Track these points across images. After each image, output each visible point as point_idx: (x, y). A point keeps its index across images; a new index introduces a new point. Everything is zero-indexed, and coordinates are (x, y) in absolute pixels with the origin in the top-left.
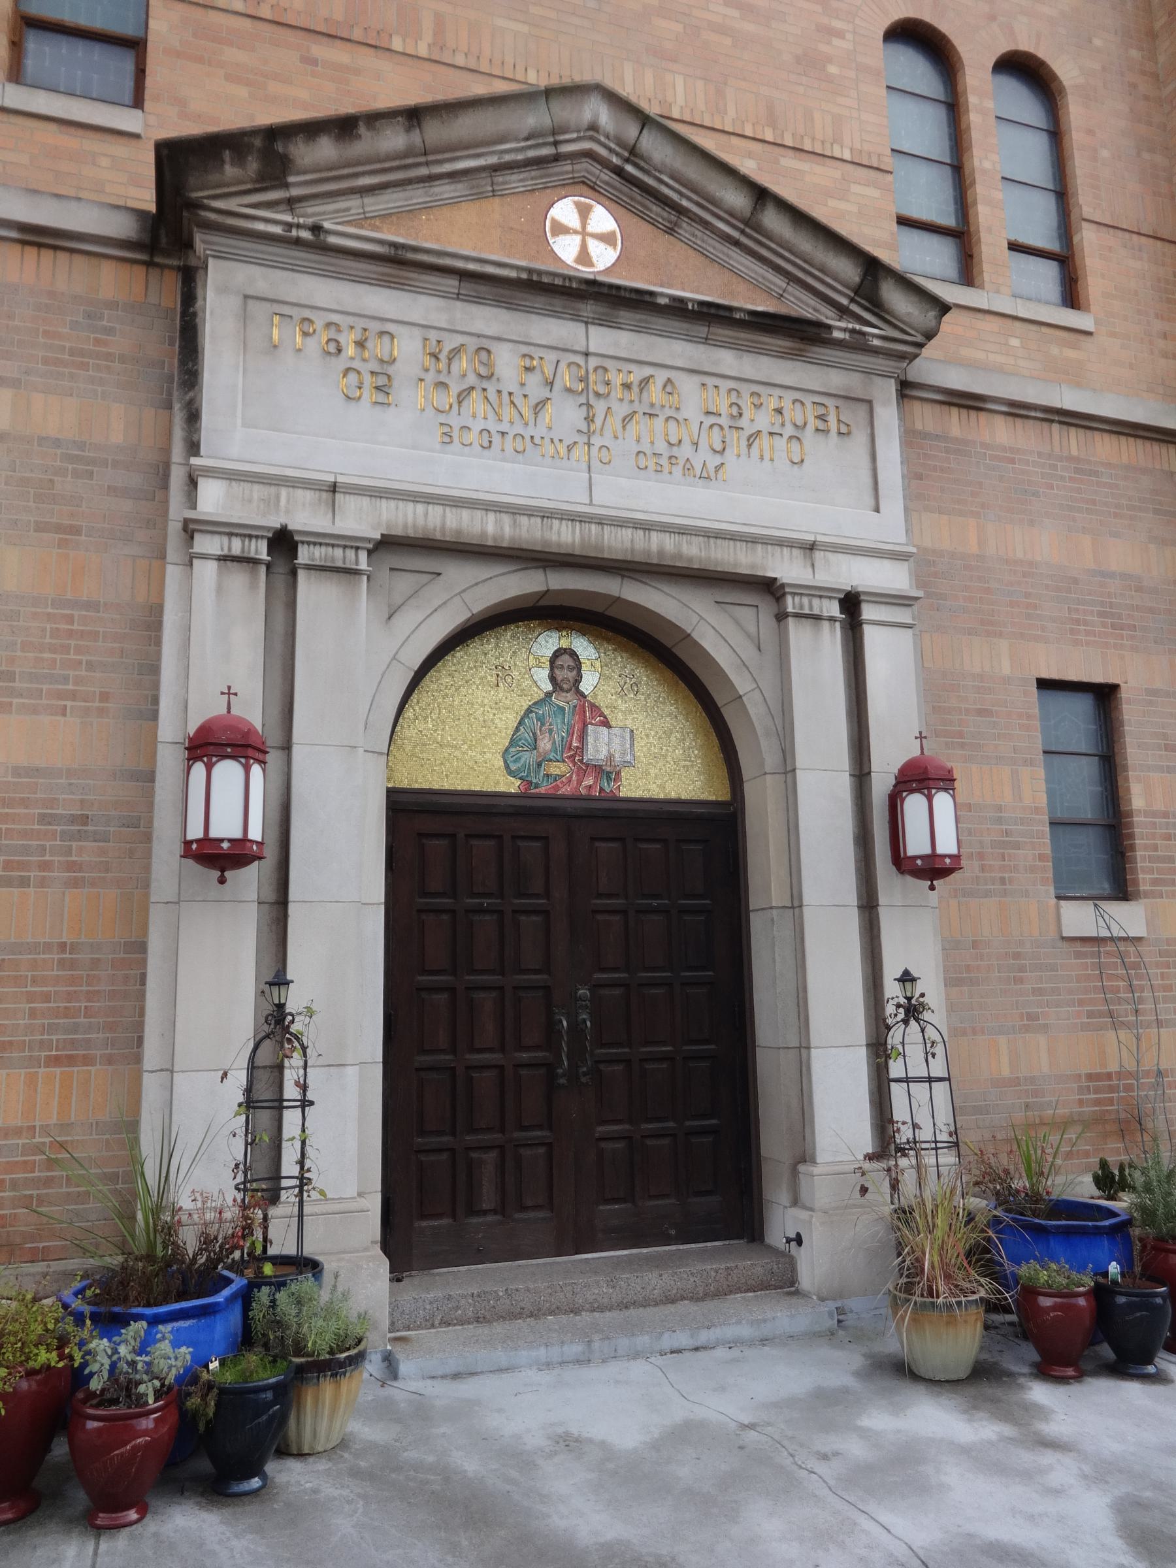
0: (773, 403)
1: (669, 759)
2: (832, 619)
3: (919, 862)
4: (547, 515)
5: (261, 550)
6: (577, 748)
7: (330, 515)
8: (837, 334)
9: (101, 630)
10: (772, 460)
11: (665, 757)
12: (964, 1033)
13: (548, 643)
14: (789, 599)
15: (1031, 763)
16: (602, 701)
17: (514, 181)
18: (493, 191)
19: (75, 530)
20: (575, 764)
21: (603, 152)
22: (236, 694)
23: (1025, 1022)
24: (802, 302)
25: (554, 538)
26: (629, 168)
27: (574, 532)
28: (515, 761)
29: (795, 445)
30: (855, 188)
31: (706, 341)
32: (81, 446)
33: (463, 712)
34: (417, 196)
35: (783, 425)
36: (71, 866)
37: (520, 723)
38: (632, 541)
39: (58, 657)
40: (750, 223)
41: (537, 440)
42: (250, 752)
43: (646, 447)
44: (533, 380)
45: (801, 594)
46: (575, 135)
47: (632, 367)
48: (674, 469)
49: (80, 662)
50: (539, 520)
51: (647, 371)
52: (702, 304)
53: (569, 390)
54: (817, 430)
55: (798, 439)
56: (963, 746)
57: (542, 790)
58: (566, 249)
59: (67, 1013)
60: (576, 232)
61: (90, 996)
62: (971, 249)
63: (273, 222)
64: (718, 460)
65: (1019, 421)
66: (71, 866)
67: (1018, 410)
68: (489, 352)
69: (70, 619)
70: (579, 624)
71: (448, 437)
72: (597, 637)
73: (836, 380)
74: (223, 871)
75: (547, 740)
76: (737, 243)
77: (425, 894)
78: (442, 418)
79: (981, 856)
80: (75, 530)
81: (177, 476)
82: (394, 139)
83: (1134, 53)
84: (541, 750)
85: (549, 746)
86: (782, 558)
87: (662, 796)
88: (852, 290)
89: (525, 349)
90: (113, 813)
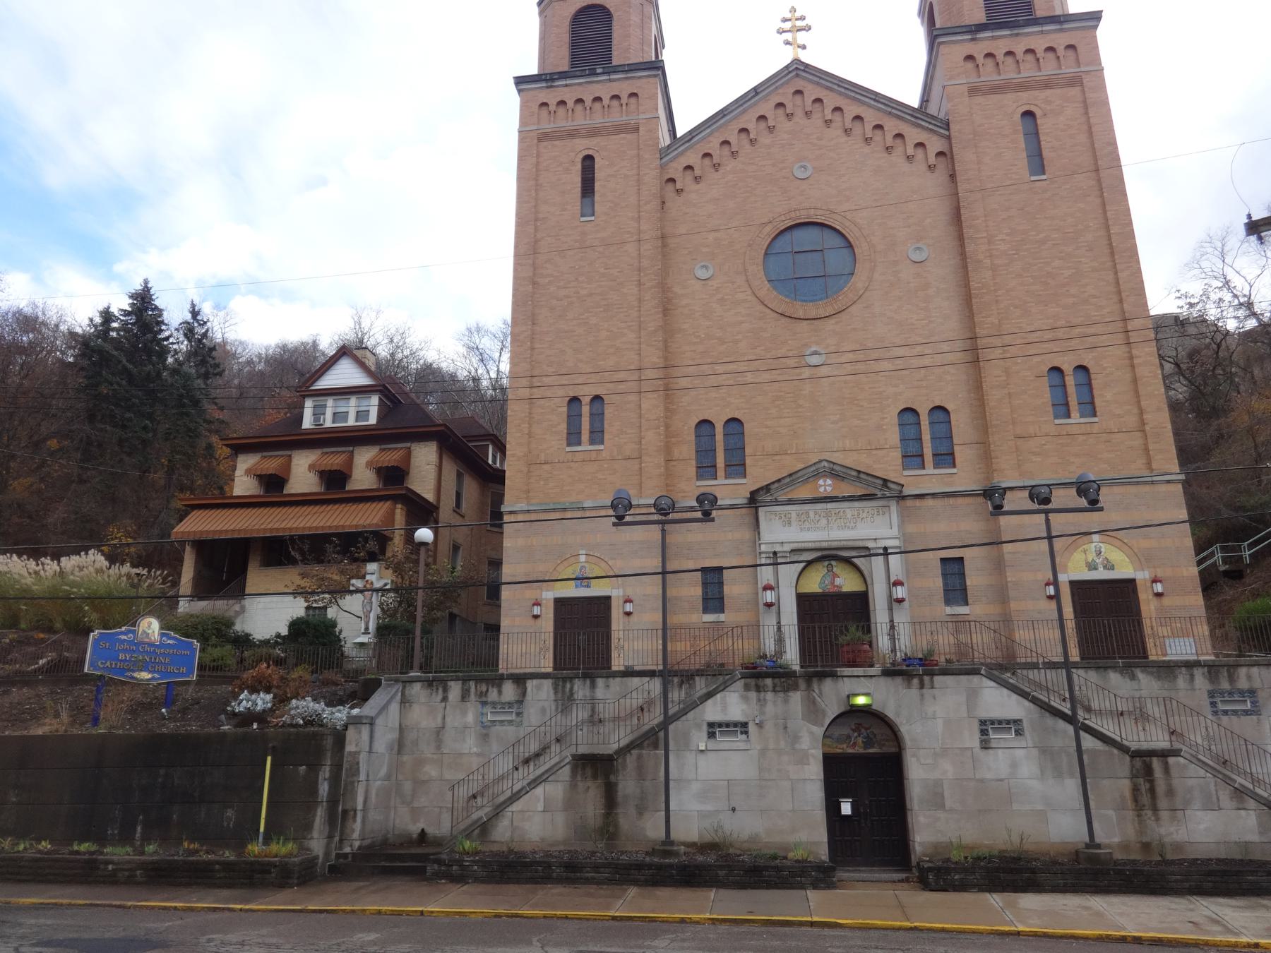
5: (771, 555)
17: (811, 479)
30: (891, 454)
34: (793, 487)
40: (858, 477)
44: (817, 516)
63: (768, 499)
67: (934, 495)
71: (801, 530)
82: (788, 480)
83: (972, 395)
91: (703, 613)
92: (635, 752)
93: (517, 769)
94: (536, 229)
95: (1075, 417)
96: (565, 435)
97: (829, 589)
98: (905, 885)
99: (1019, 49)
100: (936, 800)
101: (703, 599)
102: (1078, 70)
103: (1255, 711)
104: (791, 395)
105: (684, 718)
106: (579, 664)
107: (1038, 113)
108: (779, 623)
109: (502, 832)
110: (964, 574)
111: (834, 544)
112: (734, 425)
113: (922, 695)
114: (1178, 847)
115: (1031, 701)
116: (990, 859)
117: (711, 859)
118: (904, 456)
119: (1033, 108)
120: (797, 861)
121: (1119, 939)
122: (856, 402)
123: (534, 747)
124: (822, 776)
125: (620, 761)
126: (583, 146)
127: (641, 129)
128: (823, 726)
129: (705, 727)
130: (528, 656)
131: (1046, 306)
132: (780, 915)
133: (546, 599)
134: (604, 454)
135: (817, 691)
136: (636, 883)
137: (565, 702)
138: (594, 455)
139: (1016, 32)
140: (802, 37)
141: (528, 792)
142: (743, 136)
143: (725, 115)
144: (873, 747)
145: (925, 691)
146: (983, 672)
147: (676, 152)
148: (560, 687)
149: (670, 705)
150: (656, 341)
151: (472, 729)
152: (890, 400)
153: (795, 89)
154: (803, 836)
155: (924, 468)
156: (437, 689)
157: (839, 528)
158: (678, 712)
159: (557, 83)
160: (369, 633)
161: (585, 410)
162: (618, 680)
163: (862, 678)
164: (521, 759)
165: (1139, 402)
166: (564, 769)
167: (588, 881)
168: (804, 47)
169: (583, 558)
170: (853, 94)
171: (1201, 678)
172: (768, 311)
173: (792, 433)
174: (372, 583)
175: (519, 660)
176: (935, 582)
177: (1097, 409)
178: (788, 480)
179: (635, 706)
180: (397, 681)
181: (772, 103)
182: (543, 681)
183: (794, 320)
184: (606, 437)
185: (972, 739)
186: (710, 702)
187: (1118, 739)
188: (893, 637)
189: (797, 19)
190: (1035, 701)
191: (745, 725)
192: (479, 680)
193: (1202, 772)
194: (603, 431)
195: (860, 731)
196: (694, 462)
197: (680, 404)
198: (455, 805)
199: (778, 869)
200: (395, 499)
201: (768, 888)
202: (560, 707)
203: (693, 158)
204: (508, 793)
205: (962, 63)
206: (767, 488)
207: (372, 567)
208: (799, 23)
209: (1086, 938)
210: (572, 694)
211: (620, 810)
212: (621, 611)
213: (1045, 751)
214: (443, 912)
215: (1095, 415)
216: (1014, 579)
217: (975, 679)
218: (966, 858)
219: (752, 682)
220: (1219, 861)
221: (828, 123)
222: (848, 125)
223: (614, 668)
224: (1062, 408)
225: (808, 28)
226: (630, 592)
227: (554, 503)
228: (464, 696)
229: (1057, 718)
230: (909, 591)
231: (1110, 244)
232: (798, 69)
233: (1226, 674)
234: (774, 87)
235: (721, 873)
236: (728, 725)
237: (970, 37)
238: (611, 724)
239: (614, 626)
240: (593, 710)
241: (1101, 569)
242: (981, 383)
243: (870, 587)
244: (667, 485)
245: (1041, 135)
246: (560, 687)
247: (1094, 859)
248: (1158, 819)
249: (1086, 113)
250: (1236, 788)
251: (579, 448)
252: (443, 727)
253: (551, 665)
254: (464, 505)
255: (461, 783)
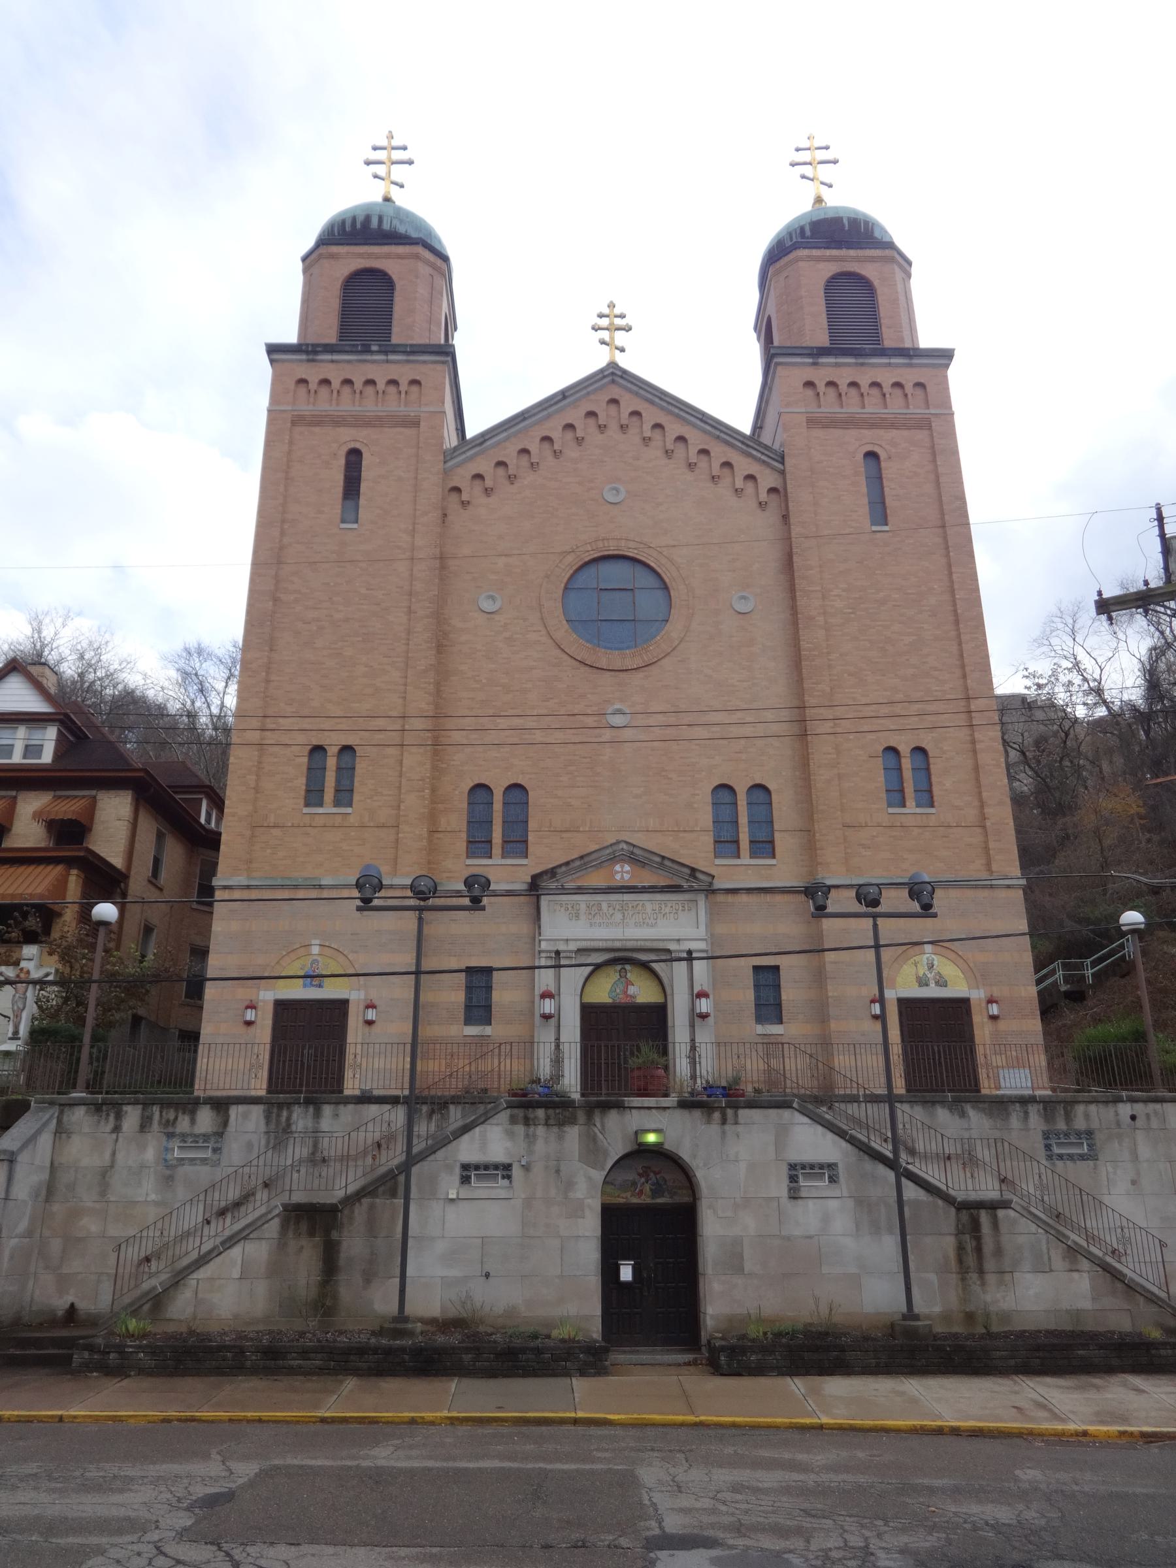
0: (669, 905)
4: (613, 940)
13: (619, 967)
17: (606, 864)
34: (584, 872)
40: (662, 864)
63: (553, 885)
67: (749, 890)
71: (591, 925)
81: (537, 940)
82: (578, 863)
83: (797, 773)
91: (466, 1024)
92: (366, 1201)
93: (208, 1223)
94: (283, 533)
95: (911, 807)
96: (303, 793)
97: (621, 999)
98: (692, 1368)
99: (864, 382)
100: (734, 1262)
101: (466, 1006)
102: (927, 411)
103: (1092, 1156)
104: (588, 760)
105: (432, 1157)
106: (301, 1085)
107: (883, 455)
108: (558, 1039)
109: (181, 1308)
110: (779, 986)
111: (629, 945)
112: (517, 793)
113: (724, 1133)
114: (1005, 1317)
115: (848, 1141)
116: (792, 1335)
117: (454, 1339)
118: (716, 842)
119: (877, 449)
120: (563, 1341)
121: (934, 1430)
122: (664, 773)
123: (233, 1194)
124: (599, 1233)
125: (346, 1212)
126: (348, 437)
127: (422, 424)
128: (603, 1169)
129: (458, 1170)
130: (234, 1074)
131: (884, 675)
132: (537, 1411)
133: (264, 1001)
134: (352, 820)
135: (598, 1125)
136: (357, 1373)
137: (279, 1135)
138: (338, 820)
139: (861, 361)
140: (620, 338)
141: (220, 1253)
142: (546, 445)
143: (525, 419)
144: (663, 1196)
145: (727, 1127)
146: (795, 1105)
147: (464, 456)
148: (274, 1115)
149: (415, 1141)
150: (426, 683)
151: (152, 1170)
152: (704, 773)
153: (610, 397)
154: (571, 1309)
155: (739, 857)
156: (108, 1115)
157: (636, 925)
158: (426, 1149)
159: (320, 357)
160: (19, 1039)
161: (331, 762)
162: (351, 1107)
163: (654, 1111)
164: (215, 1210)
165: (980, 793)
166: (271, 1222)
167: (292, 1371)
168: (622, 350)
169: (315, 950)
170: (677, 411)
171: (1036, 1117)
172: (565, 657)
174: (28, 972)
175: (222, 1079)
176: (748, 996)
177: (935, 798)
178: (578, 863)
179: (369, 1142)
180: (52, 1103)
181: (582, 411)
182: (252, 1107)
183: (595, 671)
184: (356, 797)
185: (779, 1187)
186: (466, 1137)
187: (944, 1188)
188: (693, 1061)
189: (616, 316)
190: (852, 1141)
191: (507, 1167)
192: (165, 1105)
193: (1033, 1228)
194: (352, 790)
195: (648, 1176)
196: (464, 836)
197: (452, 763)
198: (121, 1270)
199: (538, 1351)
200: (70, 862)
201: (524, 1376)
202: (272, 1141)
203: (484, 465)
204: (194, 1255)
205: (801, 389)
206: (552, 873)
207: (30, 950)
208: (618, 321)
209: (898, 1430)
210: (289, 1125)
211: (342, 1277)
212: (361, 1019)
213: (861, 1202)
214: (90, 1416)
215: (932, 806)
216: (835, 994)
217: (786, 1114)
218: (765, 1333)
219: (520, 1113)
220: (1050, 1333)
221: (646, 441)
222: (670, 446)
223: (347, 1092)
224: (897, 796)
225: (628, 329)
226: (374, 996)
227: (282, 878)
228: (145, 1125)
229: (877, 1162)
230: (716, 1005)
231: (955, 611)
232: (613, 375)
233: (1062, 1112)
234: (584, 392)
235: (467, 1358)
236: (486, 1167)
237: (810, 360)
238: (338, 1165)
239: (351, 1038)
240: (315, 1145)
241: (933, 985)
242: (808, 760)
243: (669, 998)
244: (429, 863)
245: (884, 480)
246: (274, 1115)
247: (911, 1333)
248: (983, 1284)
249: (934, 461)
250: (1069, 1246)
251: (320, 810)
252: (112, 1166)
253: (265, 1086)
254: (164, 875)
255: (131, 1240)
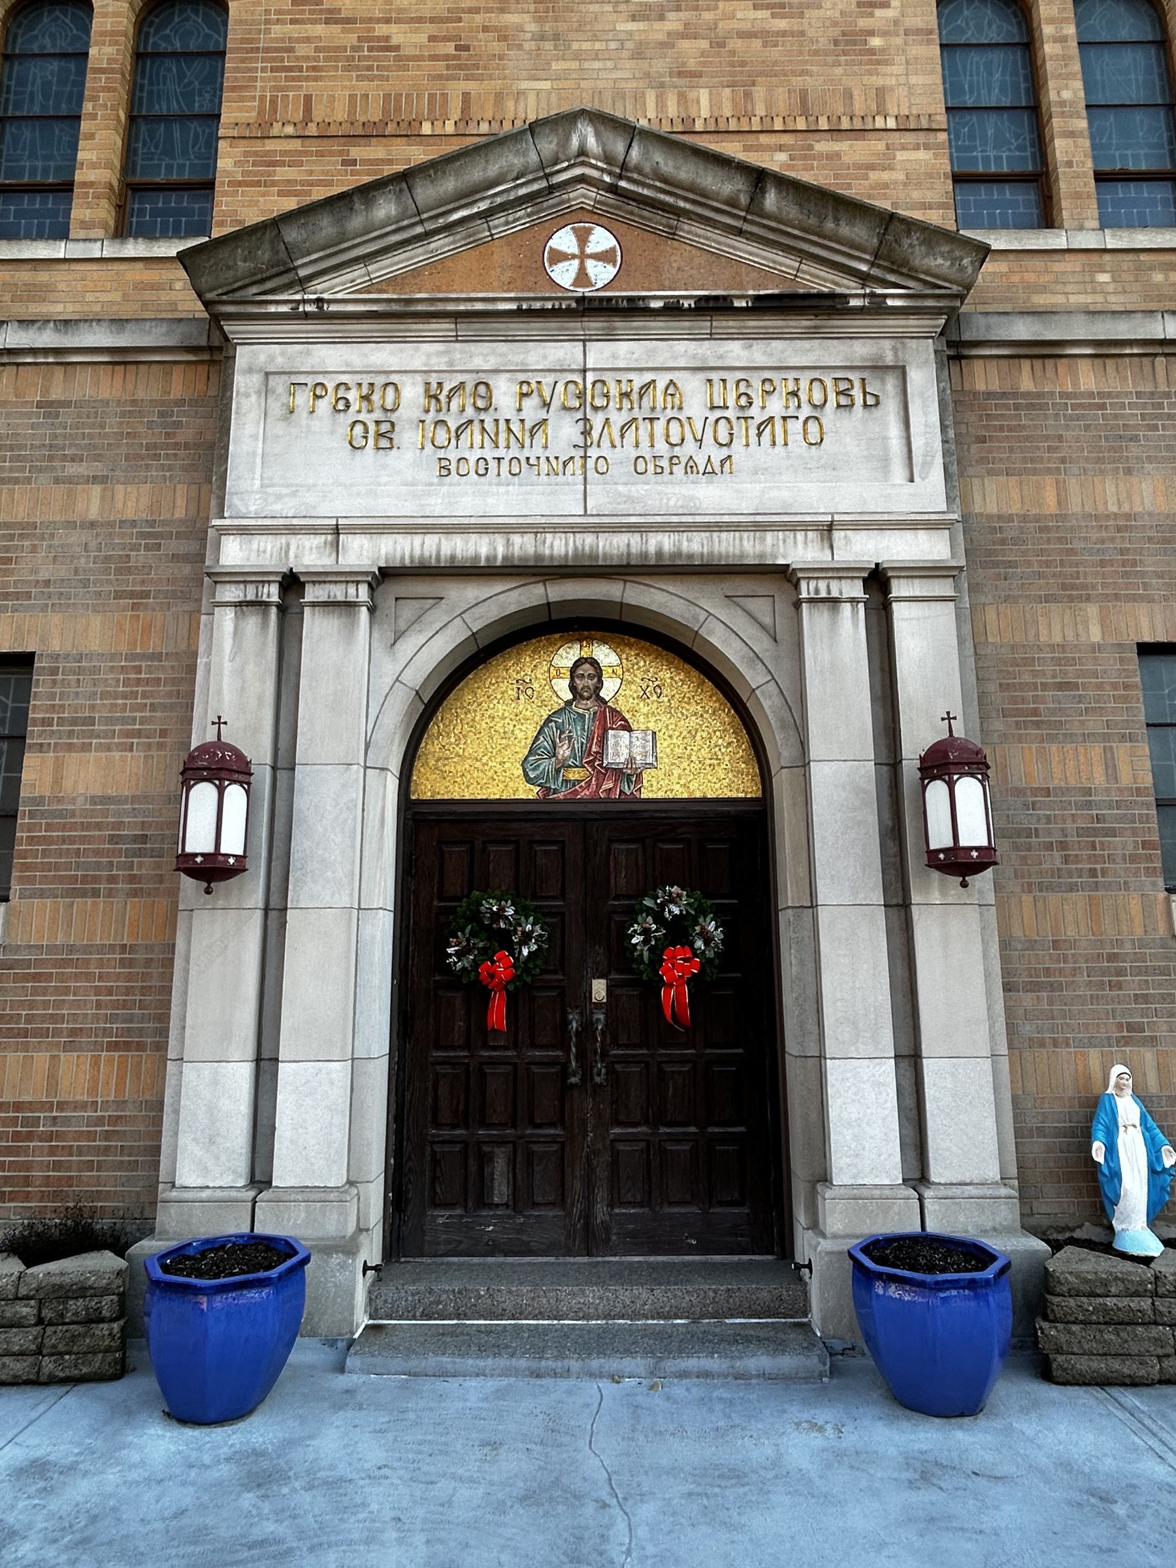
1: (693, 758)
2: (853, 601)
3: (942, 856)
4: (536, 530)
5: (272, 593)
6: (597, 753)
7: (334, 555)
8: (854, 302)
9: (163, 676)
10: (786, 444)
11: (690, 756)
12: (1042, 1044)
13: (568, 656)
14: (803, 585)
15: (1131, 738)
16: (623, 706)
18: (492, 235)
19: (146, 594)
20: (594, 768)
21: (595, 174)
22: (225, 723)
23: (1125, 1034)
24: (818, 277)
25: (547, 552)
26: (623, 184)
27: (567, 544)
28: (534, 769)
29: (813, 427)
30: (901, 156)
31: (711, 337)
32: (152, 524)
33: (484, 725)
35: (799, 406)
36: (132, 879)
37: (539, 733)
38: (628, 545)
39: (128, 702)
41: (532, 461)
42: (223, 774)
43: (645, 450)
45: (818, 578)
46: (565, 164)
47: (632, 376)
48: (675, 468)
49: (145, 705)
50: (532, 536)
51: (648, 377)
52: (700, 299)
53: (565, 408)
54: (839, 406)
55: (817, 418)
56: (1037, 725)
57: (561, 796)
58: (564, 275)
59: (125, 1005)
60: (574, 257)
61: (144, 990)
62: (1050, 189)
64: (725, 452)
65: (1110, 362)
66: (132, 879)
68: (487, 385)
69: (138, 670)
70: (599, 634)
71: (445, 470)
72: (619, 644)
73: (861, 350)
74: (209, 883)
75: (566, 747)
76: (740, 232)
77: (441, 899)
78: (441, 454)
79: (1063, 846)
80: (146, 594)
84: (560, 757)
85: (567, 753)
86: (795, 542)
87: (685, 796)
88: (870, 254)
89: (522, 377)
90: (167, 832)
173: (449, 48)
243: (782, 782)
